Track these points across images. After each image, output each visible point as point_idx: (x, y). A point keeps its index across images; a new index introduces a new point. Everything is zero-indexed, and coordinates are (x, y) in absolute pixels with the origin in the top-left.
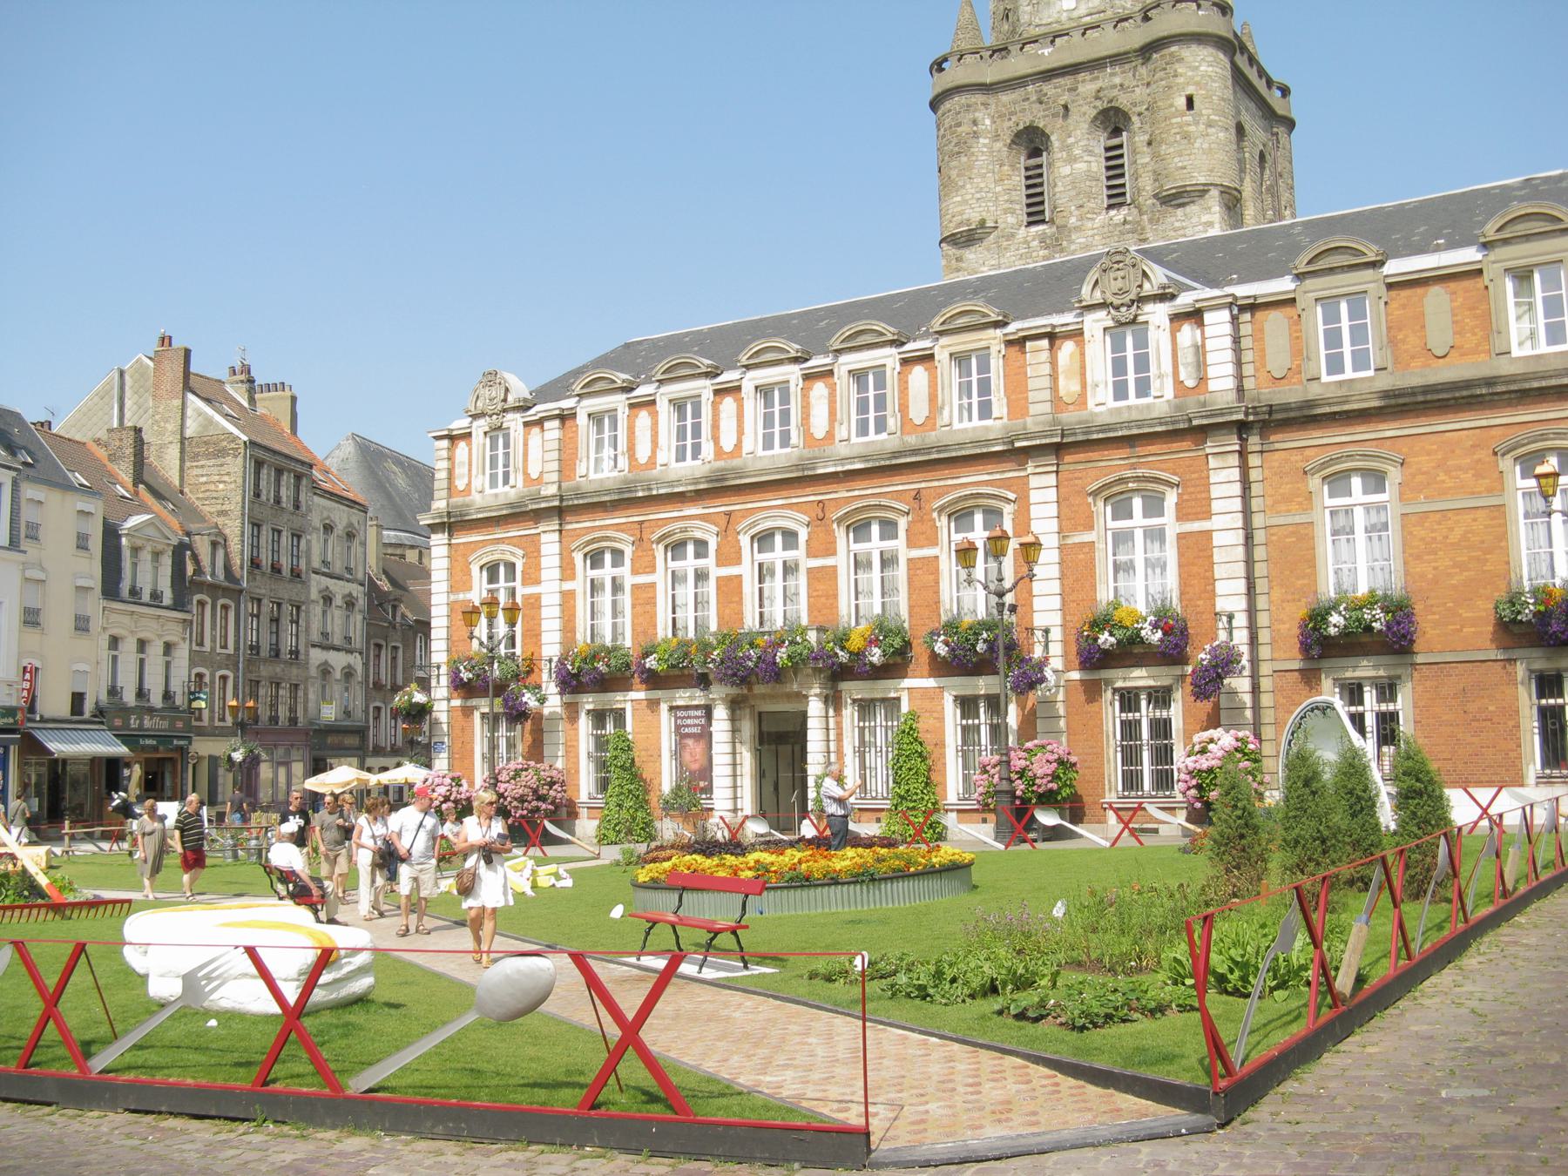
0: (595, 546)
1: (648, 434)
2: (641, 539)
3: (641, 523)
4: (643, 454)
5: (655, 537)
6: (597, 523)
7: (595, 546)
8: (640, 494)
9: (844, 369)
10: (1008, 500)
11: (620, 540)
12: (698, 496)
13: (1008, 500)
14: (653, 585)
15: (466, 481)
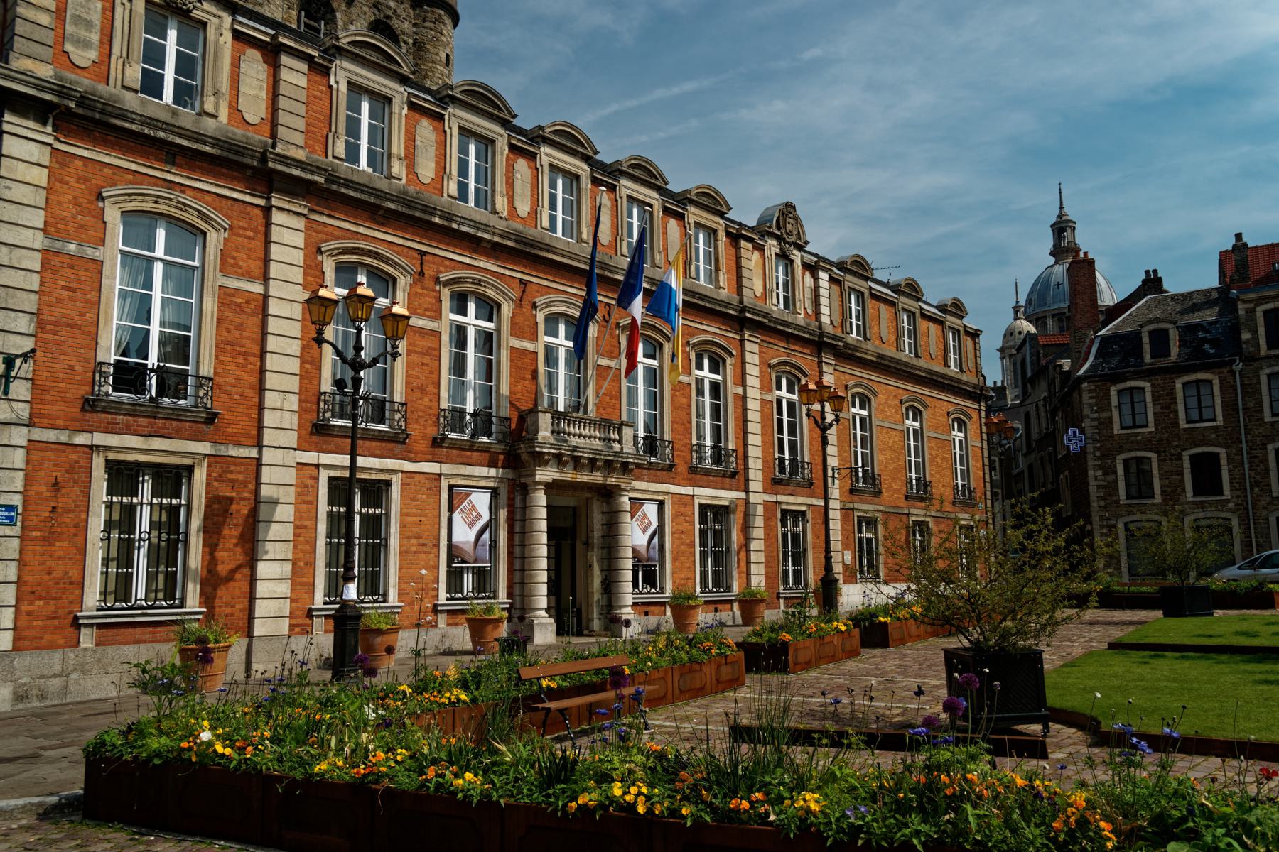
0: (355, 258)
1: (432, 151)
2: (422, 273)
3: (425, 253)
4: (427, 171)
5: (444, 277)
6: (361, 230)
7: (355, 258)
8: (437, 220)
9: (624, 192)
10: (731, 355)
11: (394, 264)
12: (495, 251)
13: (731, 355)
14: (438, 334)
15: (93, 55)
